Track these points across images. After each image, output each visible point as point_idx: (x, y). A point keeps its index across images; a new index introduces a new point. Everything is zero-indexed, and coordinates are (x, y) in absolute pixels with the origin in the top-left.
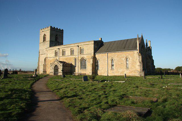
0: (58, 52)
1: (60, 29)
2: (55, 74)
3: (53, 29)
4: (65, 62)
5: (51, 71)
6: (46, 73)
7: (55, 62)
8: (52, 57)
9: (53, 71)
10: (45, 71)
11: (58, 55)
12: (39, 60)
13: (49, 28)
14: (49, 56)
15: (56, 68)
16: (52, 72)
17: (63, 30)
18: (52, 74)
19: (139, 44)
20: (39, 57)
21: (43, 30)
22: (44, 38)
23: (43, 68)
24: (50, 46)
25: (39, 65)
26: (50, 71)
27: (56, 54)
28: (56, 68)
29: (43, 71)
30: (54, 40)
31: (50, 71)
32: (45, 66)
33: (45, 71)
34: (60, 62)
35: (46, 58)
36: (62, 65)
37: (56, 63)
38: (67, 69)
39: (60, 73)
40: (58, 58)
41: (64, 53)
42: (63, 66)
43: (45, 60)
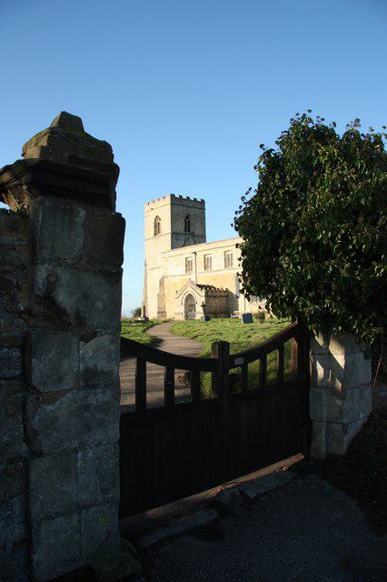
0: (194, 262)
1: (195, 199)
2: (187, 316)
3: (176, 201)
4: (210, 287)
5: (177, 311)
6: (165, 316)
7: (186, 286)
8: (177, 274)
9: (182, 309)
10: (162, 312)
11: (194, 265)
12: (146, 285)
13: (168, 200)
14: (170, 272)
15: (189, 303)
16: (178, 314)
17: (203, 202)
18: (181, 318)
19: (275, 475)
20: (146, 277)
21: (152, 205)
22: (155, 227)
23: (156, 304)
24: (173, 247)
25: (146, 297)
26: (175, 310)
27: (188, 266)
28: (189, 302)
29: (159, 312)
30: (181, 228)
31: (175, 310)
32: (161, 297)
33: (162, 312)
34: (199, 286)
35: (163, 278)
36: (203, 293)
37: (190, 290)
38: (217, 303)
39: (199, 313)
40: (194, 276)
41: (207, 264)
42: (207, 296)
43: (162, 283)
